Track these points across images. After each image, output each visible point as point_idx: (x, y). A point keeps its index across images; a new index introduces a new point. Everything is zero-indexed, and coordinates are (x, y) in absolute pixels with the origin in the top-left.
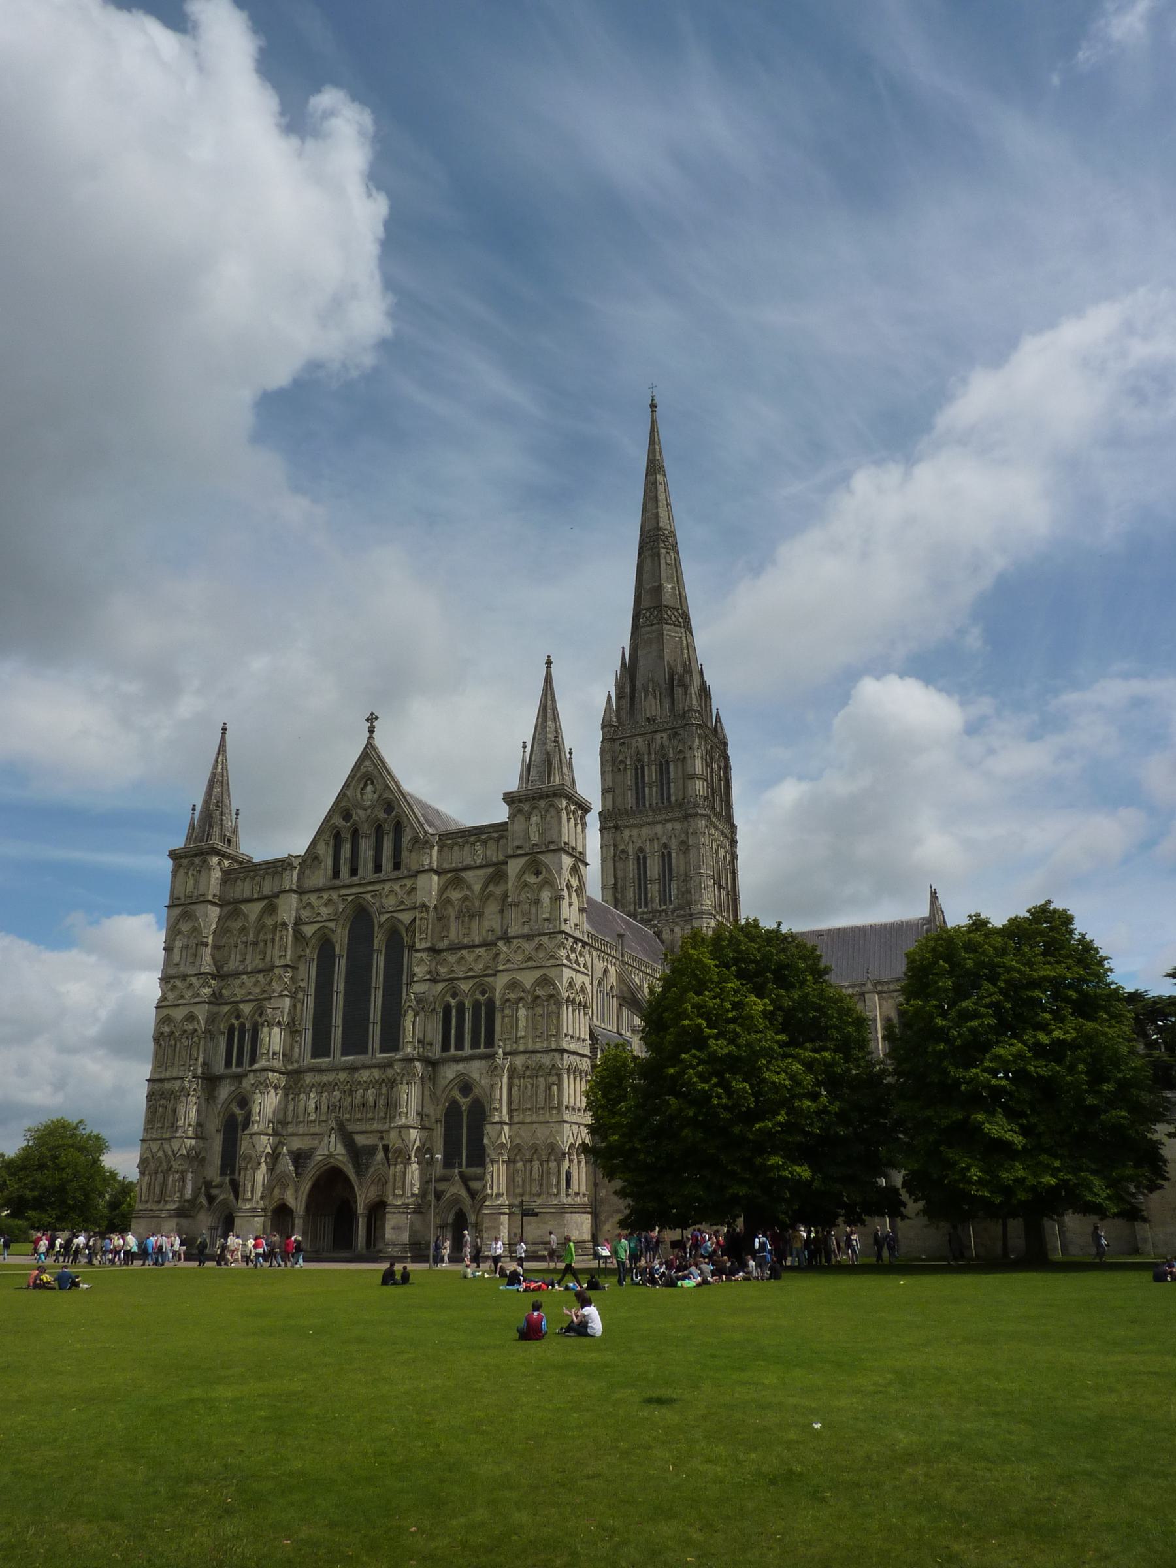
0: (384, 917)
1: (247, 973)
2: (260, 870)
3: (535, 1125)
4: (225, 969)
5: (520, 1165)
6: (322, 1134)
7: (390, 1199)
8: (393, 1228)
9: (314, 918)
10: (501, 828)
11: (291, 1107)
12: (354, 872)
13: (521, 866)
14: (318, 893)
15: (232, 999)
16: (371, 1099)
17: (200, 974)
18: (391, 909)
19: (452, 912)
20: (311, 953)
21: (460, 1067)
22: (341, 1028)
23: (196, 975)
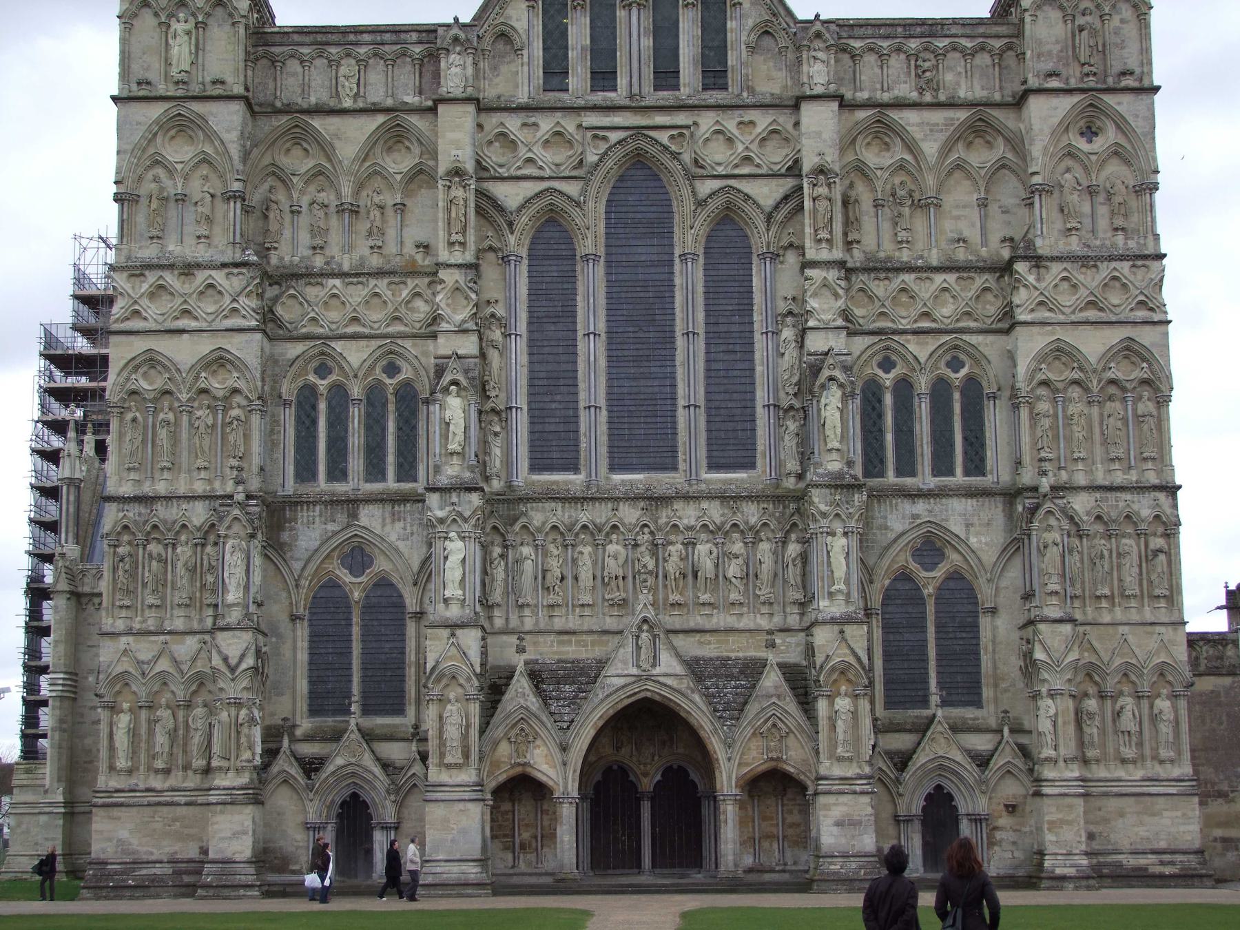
0: (706, 187)
1: (342, 275)
2: (356, 44)
3: (1121, 629)
4: (274, 260)
5: (1092, 704)
6: (621, 632)
7: (827, 767)
8: (838, 824)
9: (519, 168)
10: (981, 30)
11: (499, 572)
12: (603, 77)
13: (1061, 113)
14: (523, 115)
15: (304, 330)
16: (707, 565)
17: (237, 265)
18: (720, 170)
19: (864, 196)
20: (517, 243)
21: (921, 507)
22: (604, 413)
23: (224, 266)
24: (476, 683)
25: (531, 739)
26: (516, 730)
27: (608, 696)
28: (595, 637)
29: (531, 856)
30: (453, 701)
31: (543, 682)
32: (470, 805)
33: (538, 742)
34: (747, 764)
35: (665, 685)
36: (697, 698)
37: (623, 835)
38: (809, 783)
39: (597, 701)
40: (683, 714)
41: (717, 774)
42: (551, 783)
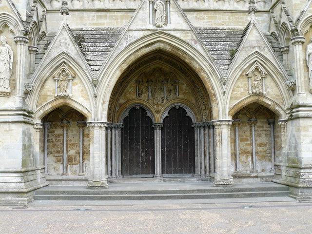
24: (22, 28)
25: (70, 77)
26: (59, 71)
27: (130, 45)
28: (124, 13)
29: (76, 167)
30: (4, 43)
31: (84, 41)
32: (13, 126)
33: (76, 81)
34: (237, 98)
35: (175, 37)
36: (198, 47)
37: (143, 152)
38: (282, 112)
39: (122, 48)
40: (187, 61)
41: (214, 105)
42: (85, 112)
